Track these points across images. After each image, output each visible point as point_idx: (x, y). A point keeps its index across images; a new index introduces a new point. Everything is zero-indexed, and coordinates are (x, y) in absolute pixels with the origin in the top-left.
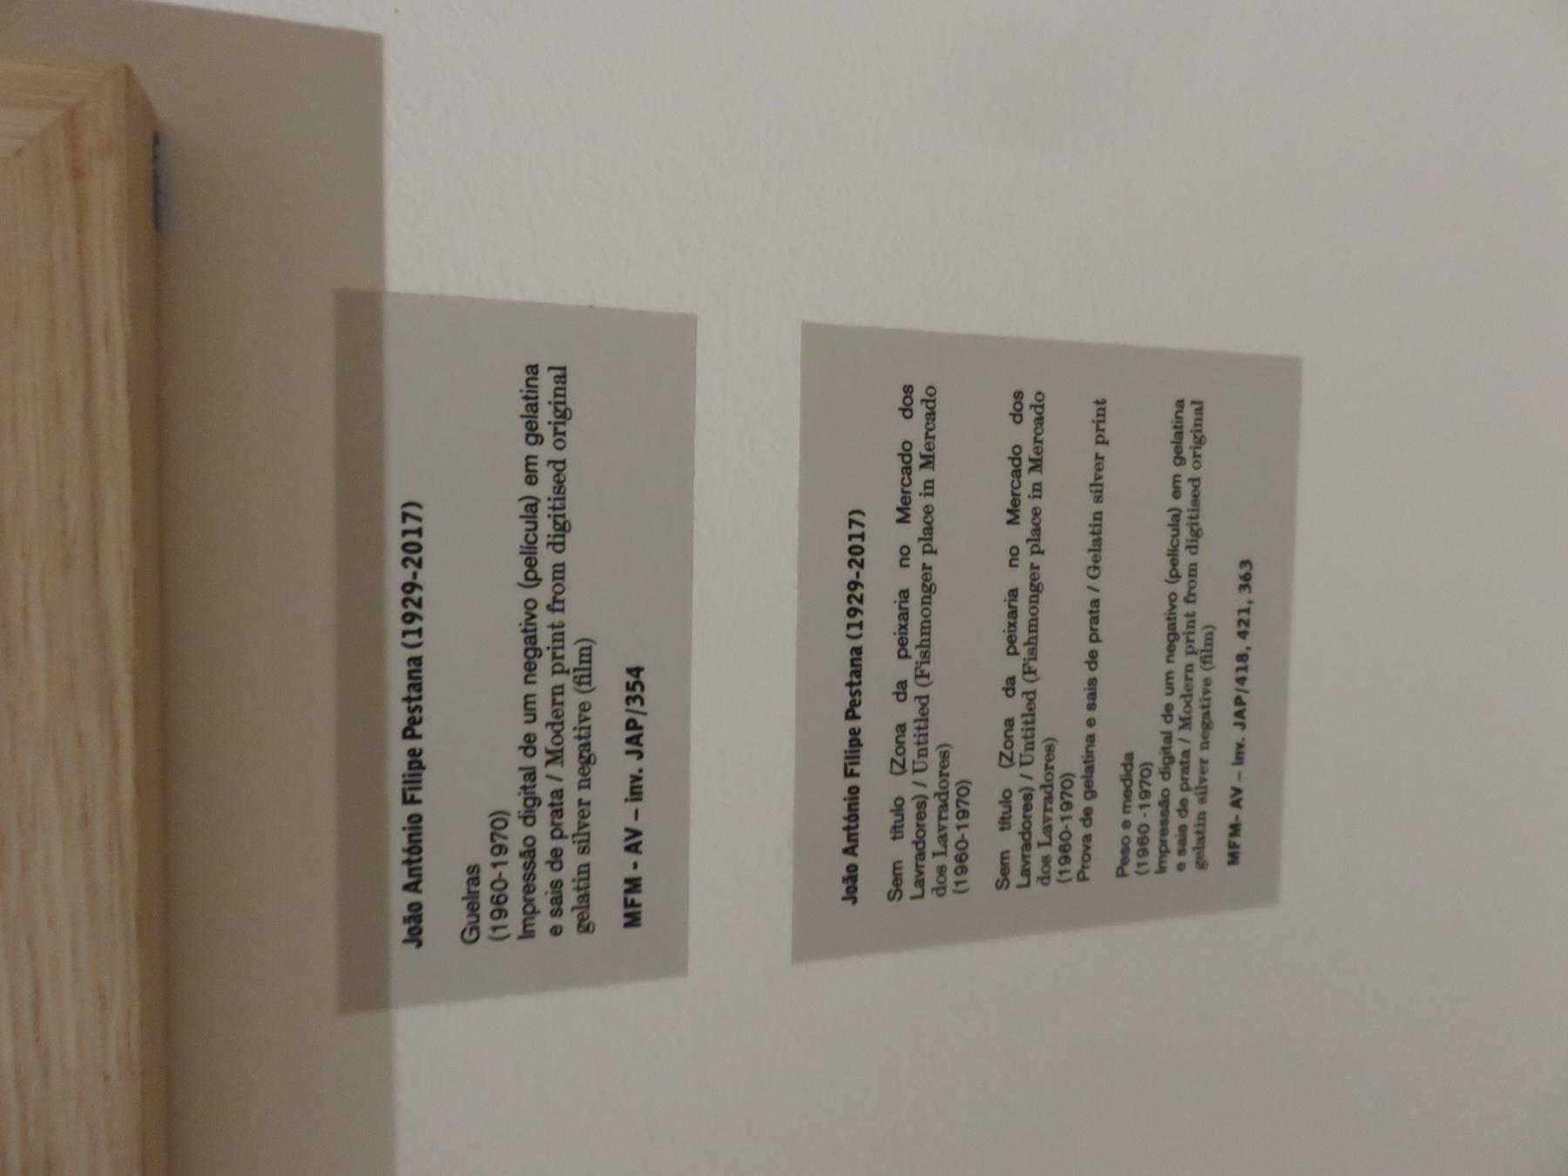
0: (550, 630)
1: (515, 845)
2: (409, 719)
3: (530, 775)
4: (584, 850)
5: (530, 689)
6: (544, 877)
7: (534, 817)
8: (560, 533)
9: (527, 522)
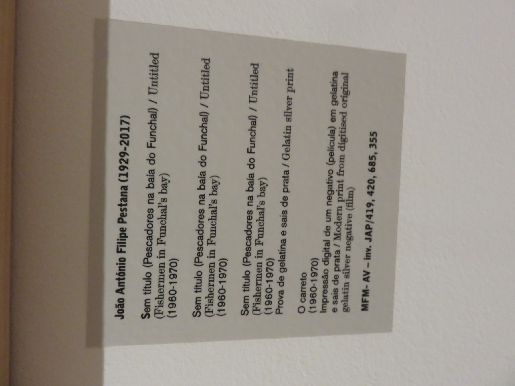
0: (338, 183)
1: (320, 273)
2: (121, 214)
3: (327, 243)
4: (347, 277)
5: (329, 207)
6: (331, 287)
7: (328, 261)
8: (343, 142)
9: (331, 137)
